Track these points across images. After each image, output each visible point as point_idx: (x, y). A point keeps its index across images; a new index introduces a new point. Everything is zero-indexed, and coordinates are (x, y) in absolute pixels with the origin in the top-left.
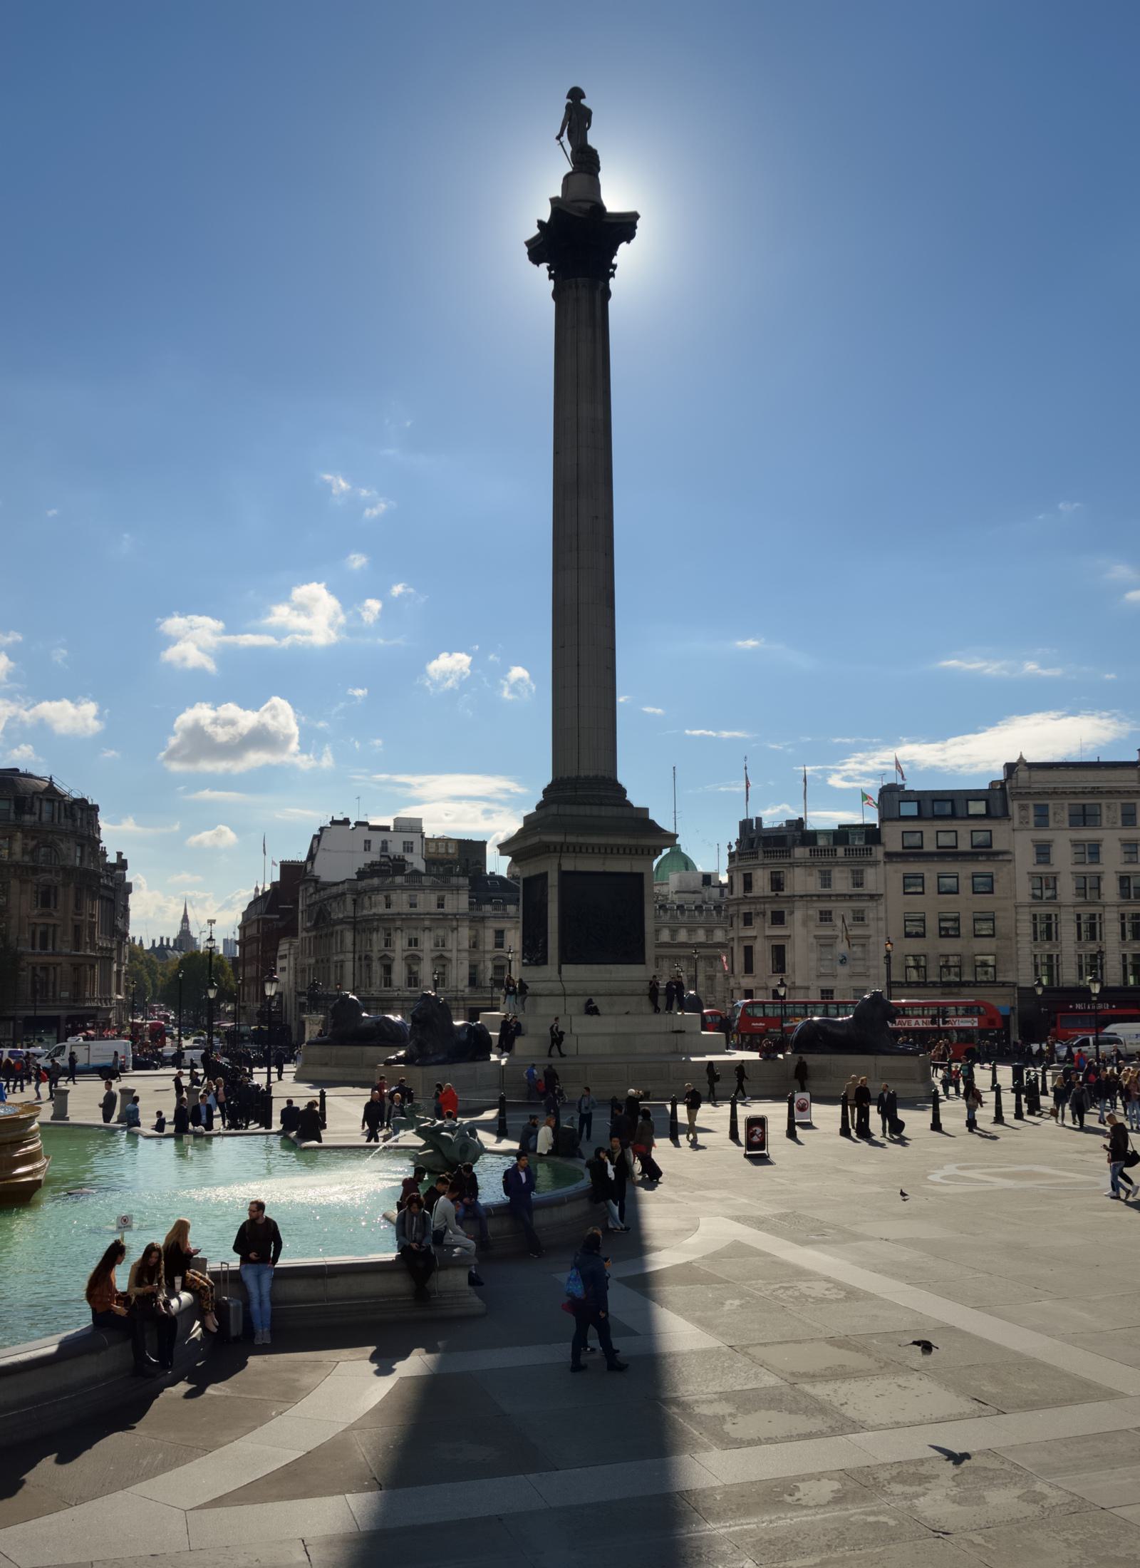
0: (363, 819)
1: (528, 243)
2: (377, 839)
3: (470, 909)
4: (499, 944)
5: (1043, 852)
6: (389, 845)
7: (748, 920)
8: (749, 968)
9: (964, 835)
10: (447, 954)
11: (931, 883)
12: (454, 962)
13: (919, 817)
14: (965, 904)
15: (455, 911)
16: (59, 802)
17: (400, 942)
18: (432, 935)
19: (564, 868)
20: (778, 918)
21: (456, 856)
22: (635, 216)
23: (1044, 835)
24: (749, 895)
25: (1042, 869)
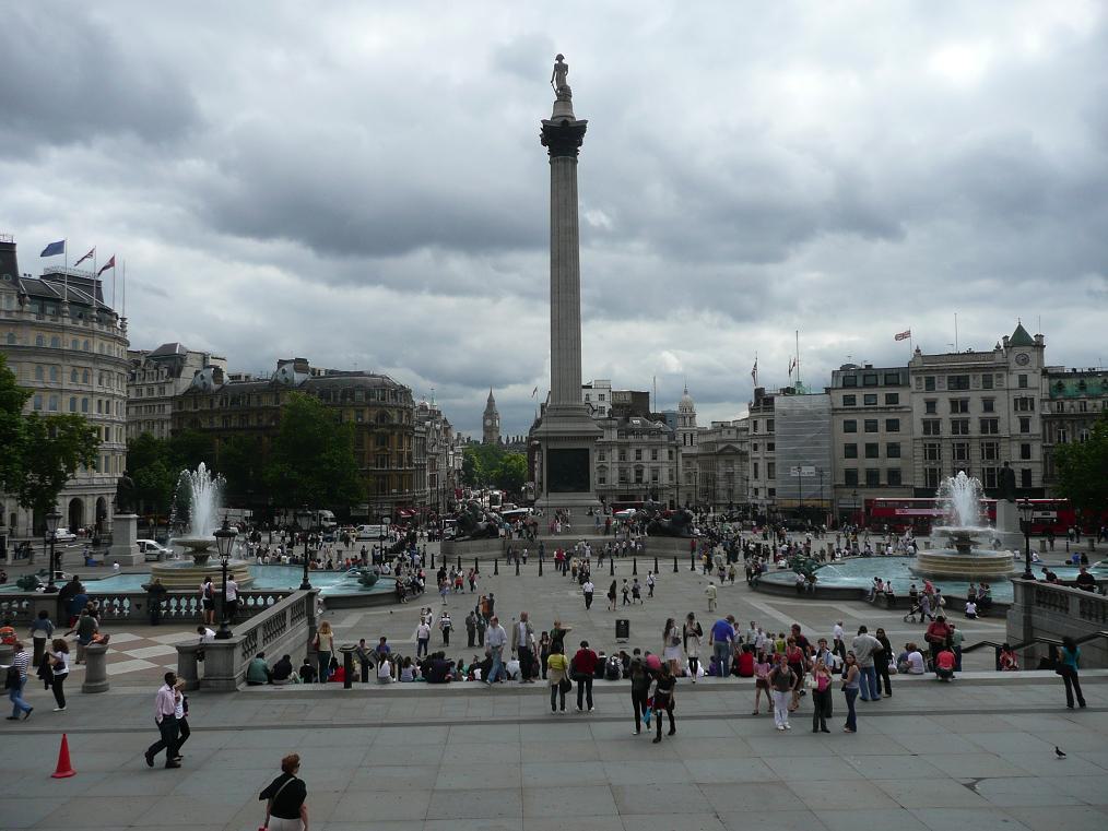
4: (639, 458)
5: (931, 406)
7: (755, 447)
8: (756, 477)
11: (861, 425)
13: (855, 386)
14: (882, 437)
22: (586, 122)
23: (932, 396)
25: (930, 416)
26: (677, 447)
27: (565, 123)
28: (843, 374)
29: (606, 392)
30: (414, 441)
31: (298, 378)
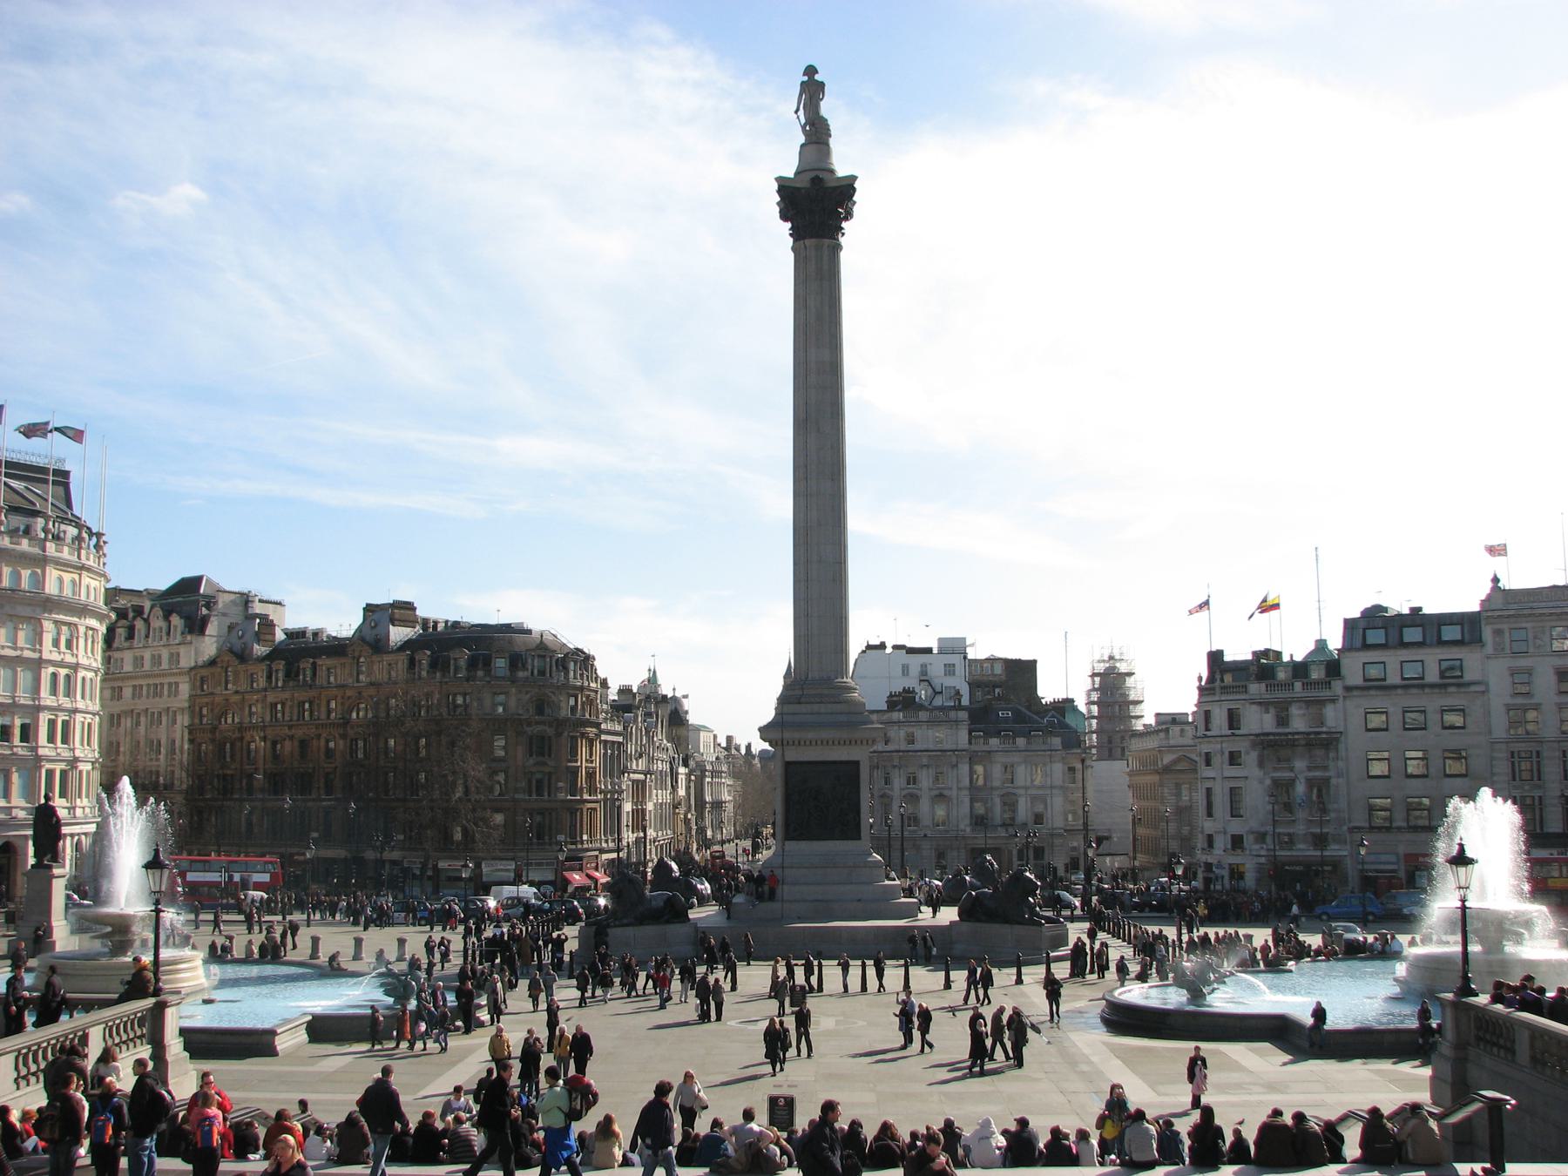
0: (900, 643)
1: (778, 204)
2: (916, 661)
3: (970, 743)
6: (929, 666)
8: (1210, 814)
9: (1431, 662)
10: (946, 792)
12: (955, 802)
15: (954, 747)
16: (551, 657)
17: (898, 782)
18: (932, 771)
19: (787, 759)
20: (1234, 759)
21: (1004, 678)
22: (854, 178)
23: (1523, 663)
24: (1208, 733)
26: (1083, 761)
27: (817, 181)
28: (1362, 624)
29: (956, 659)
30: (598, 747)
31: (398, 634)
